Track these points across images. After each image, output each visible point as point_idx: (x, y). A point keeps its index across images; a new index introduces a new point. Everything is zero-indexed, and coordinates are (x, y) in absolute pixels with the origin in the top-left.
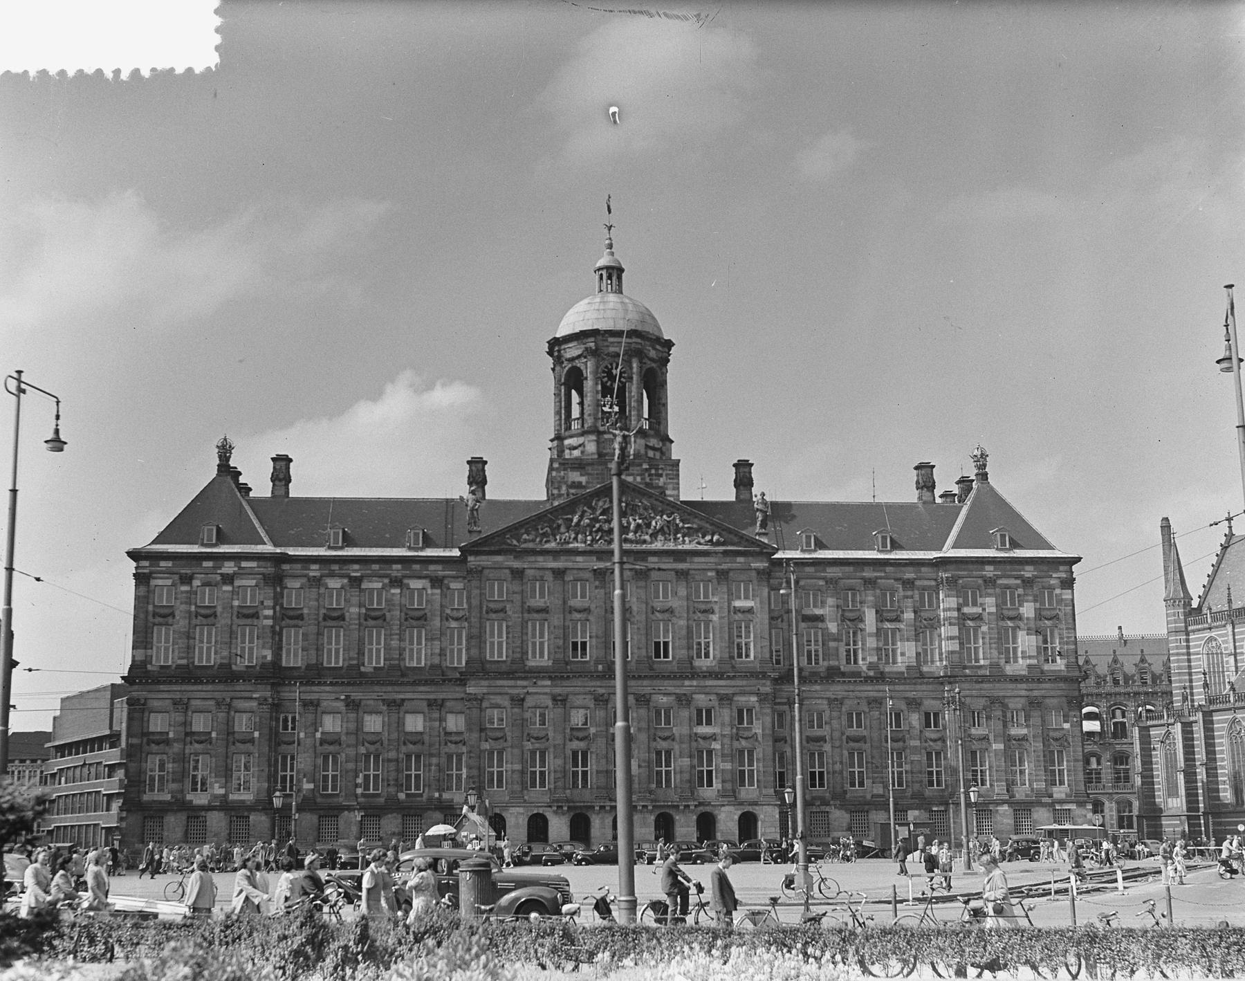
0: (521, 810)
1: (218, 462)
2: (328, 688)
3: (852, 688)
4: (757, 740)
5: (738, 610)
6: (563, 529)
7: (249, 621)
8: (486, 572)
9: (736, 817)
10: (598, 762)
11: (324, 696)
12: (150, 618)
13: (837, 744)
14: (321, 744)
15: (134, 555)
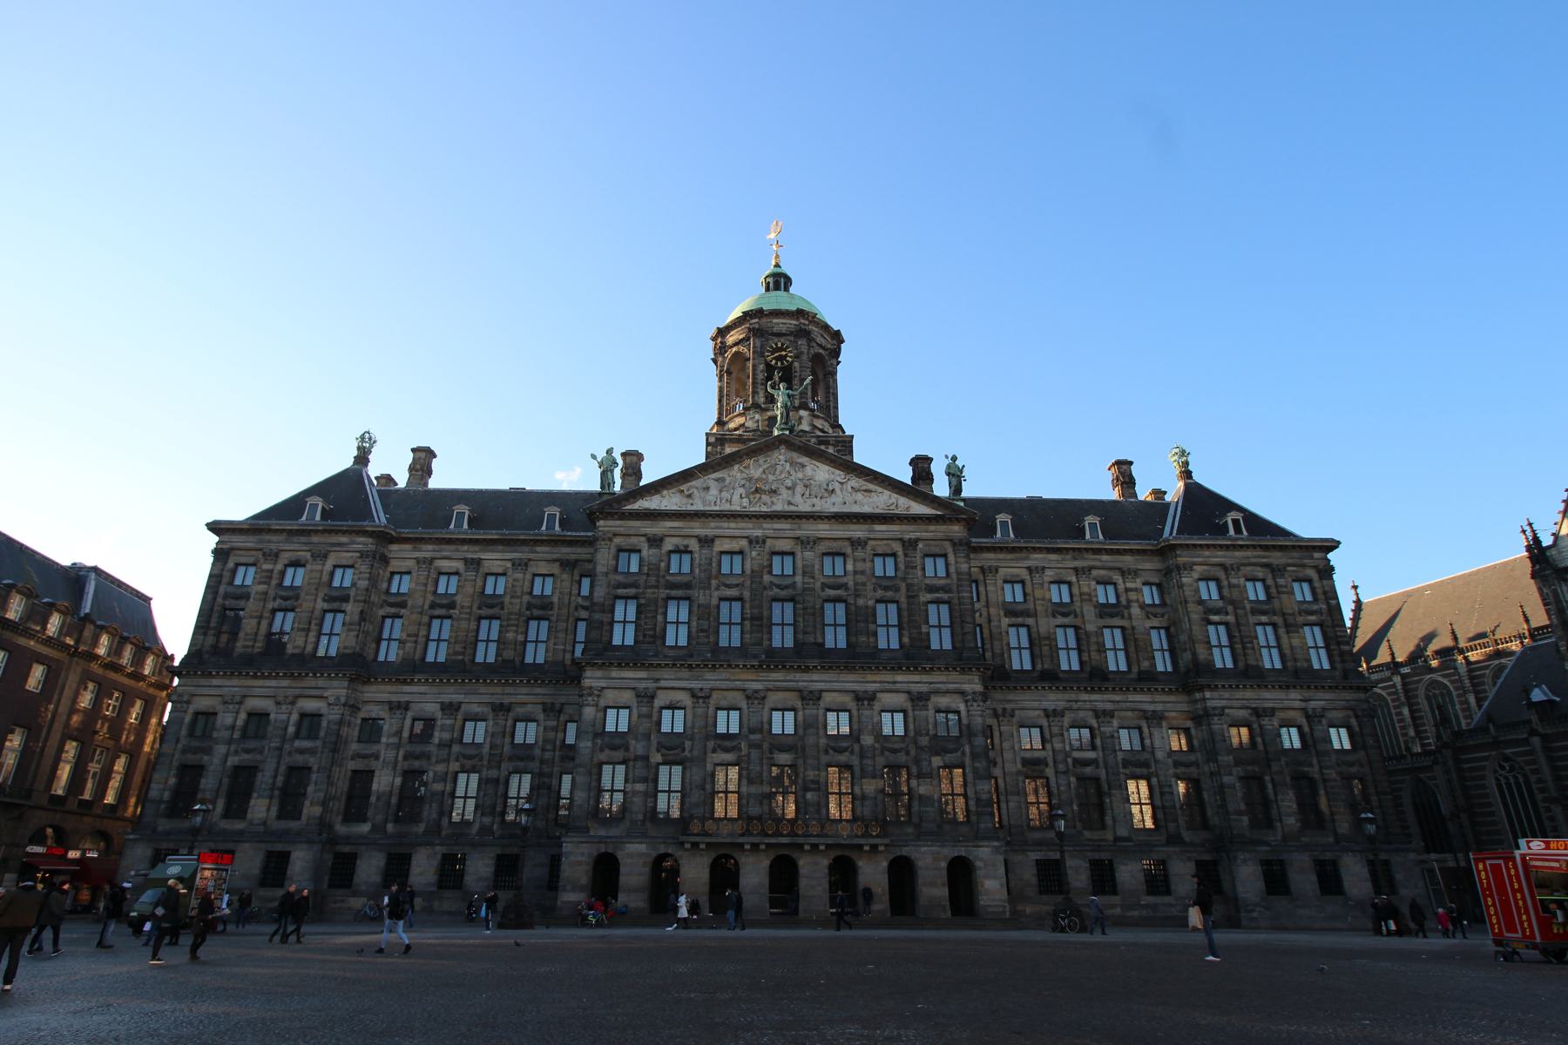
0: (642, 848)
1: (355, 453)
2: (423, 689)
3: (1073, 697)
4: (963, 753)
5: (931, 589)
6: (714, 492)
7: (335, 605)
8: (617, 540)
9: (944, 864)
10: (751, 782)
11: (416, 698)
12: (220, 600)
13: (1061, 767)
14: (406, 758)
15: (214, 527)
